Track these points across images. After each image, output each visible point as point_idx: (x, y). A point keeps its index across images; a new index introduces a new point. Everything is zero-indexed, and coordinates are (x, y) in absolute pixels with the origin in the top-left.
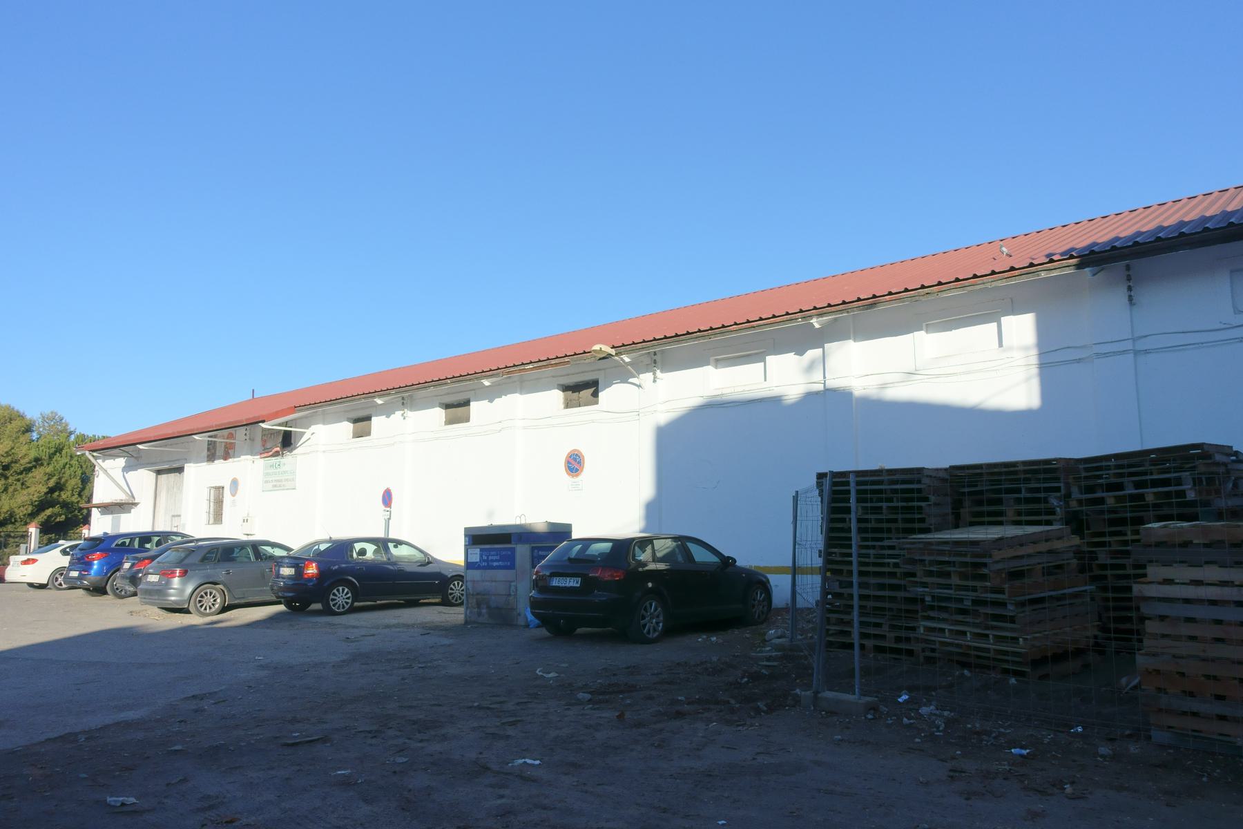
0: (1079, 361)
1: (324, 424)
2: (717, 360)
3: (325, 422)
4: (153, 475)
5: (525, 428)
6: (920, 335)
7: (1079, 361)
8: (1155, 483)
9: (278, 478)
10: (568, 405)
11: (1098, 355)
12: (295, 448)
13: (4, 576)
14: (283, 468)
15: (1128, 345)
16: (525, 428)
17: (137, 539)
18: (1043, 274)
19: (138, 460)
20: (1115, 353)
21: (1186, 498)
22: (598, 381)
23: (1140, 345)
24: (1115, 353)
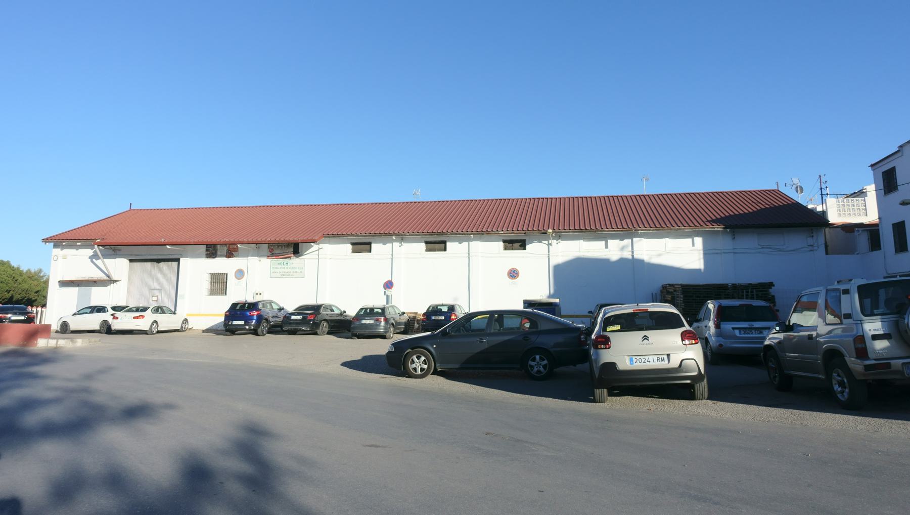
0: (717, 253)
1: (329, 244)
2: (584, 238)
3: (329, 243)
4: (128, 262)
5: (482, 257)
6: (667, 239)
7: (717, 253)
8: (761, 291)
9: (288, 271)
10: (506, 249)
11: (724, 253)
12: (302, 255)
13: (888, 341)
14: (290, 266)
15: (732, 251)
16: (482, 257)
17: (369, 309)
18: (716, 229)
19: (115, 252)
20: (729, 253)
21: (843, 294)
22: (896, 252)
23: (735, 251)
24: (729, 253)
